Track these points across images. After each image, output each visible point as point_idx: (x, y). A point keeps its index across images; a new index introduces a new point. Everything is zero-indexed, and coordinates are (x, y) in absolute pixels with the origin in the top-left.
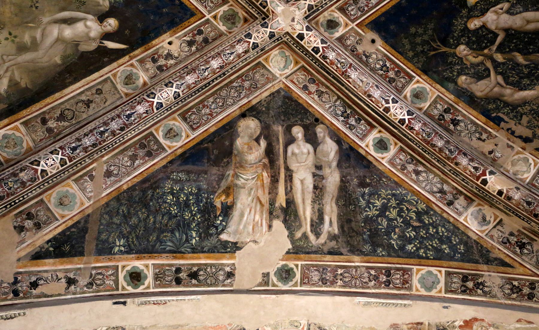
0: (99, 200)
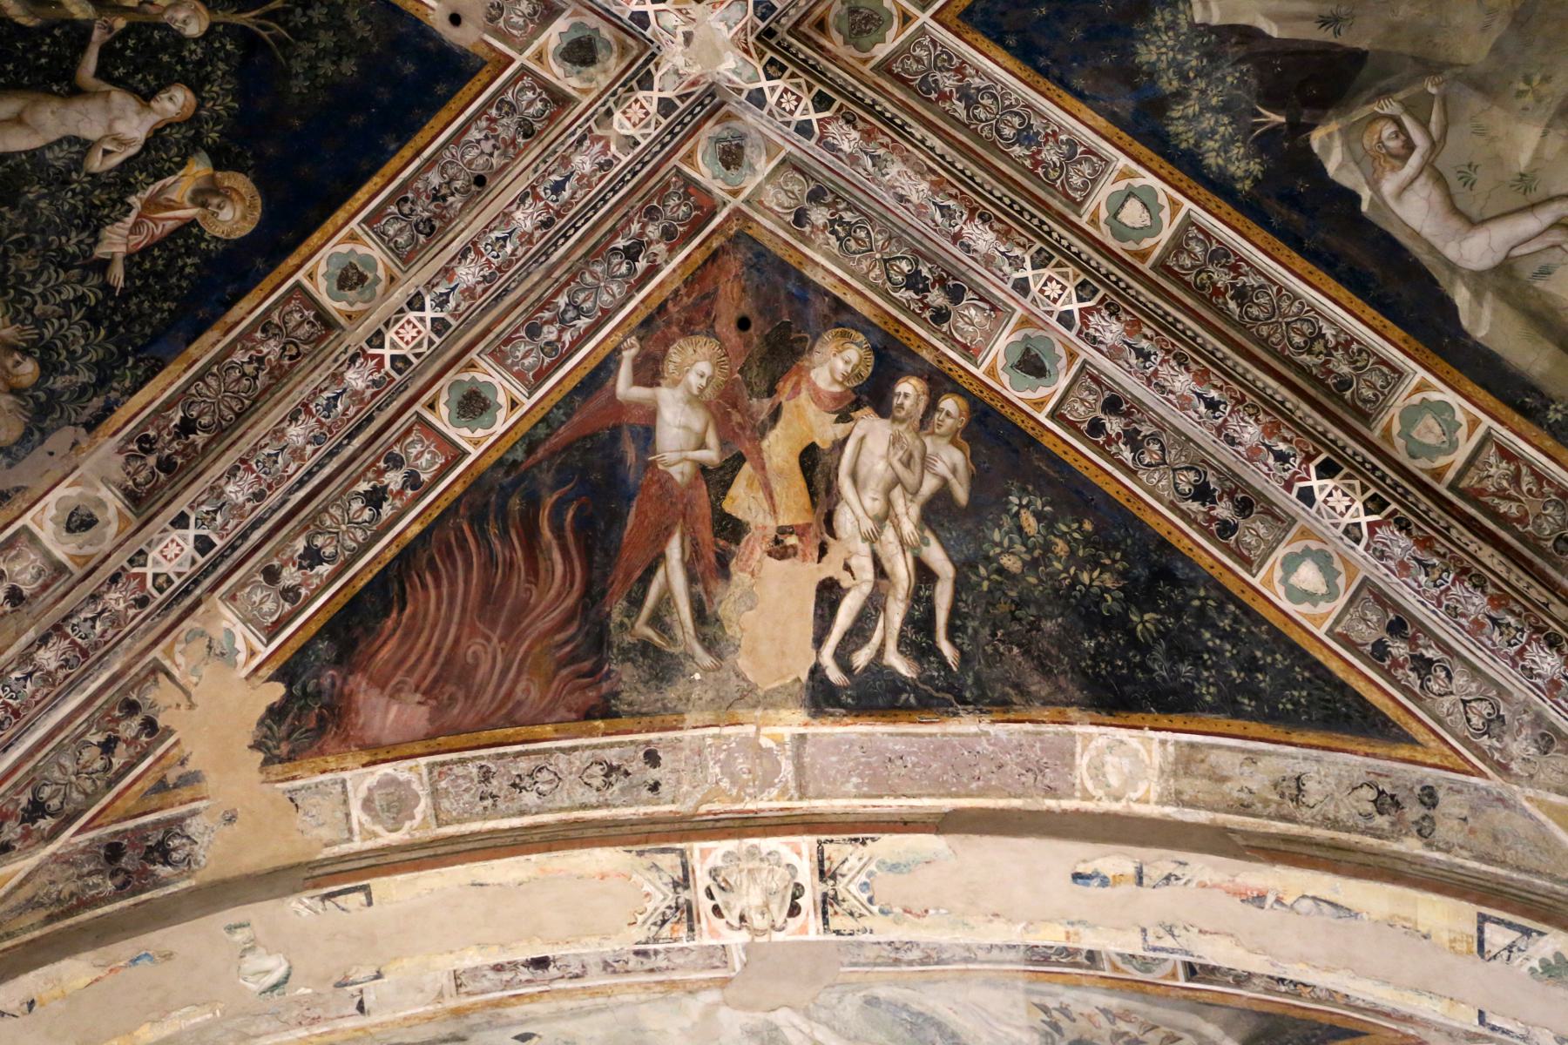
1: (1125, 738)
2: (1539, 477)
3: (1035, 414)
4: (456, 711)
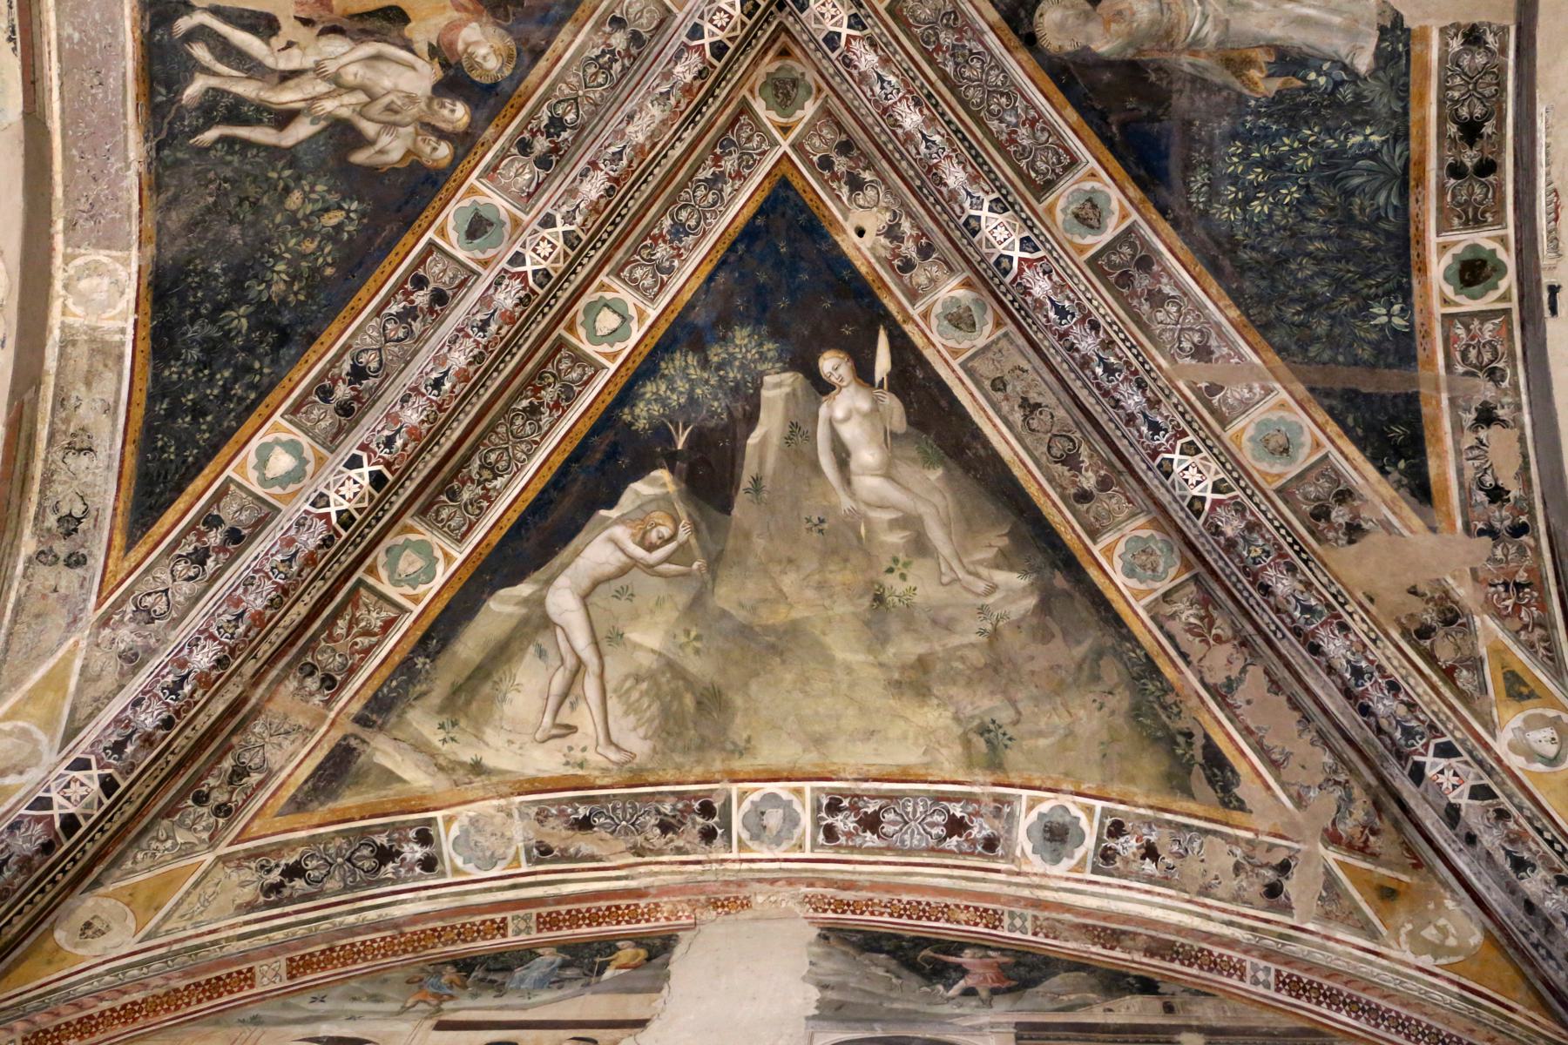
0: (1271, 370)
1: (126, 297)
2: (367, 651)
3: (433, 228)
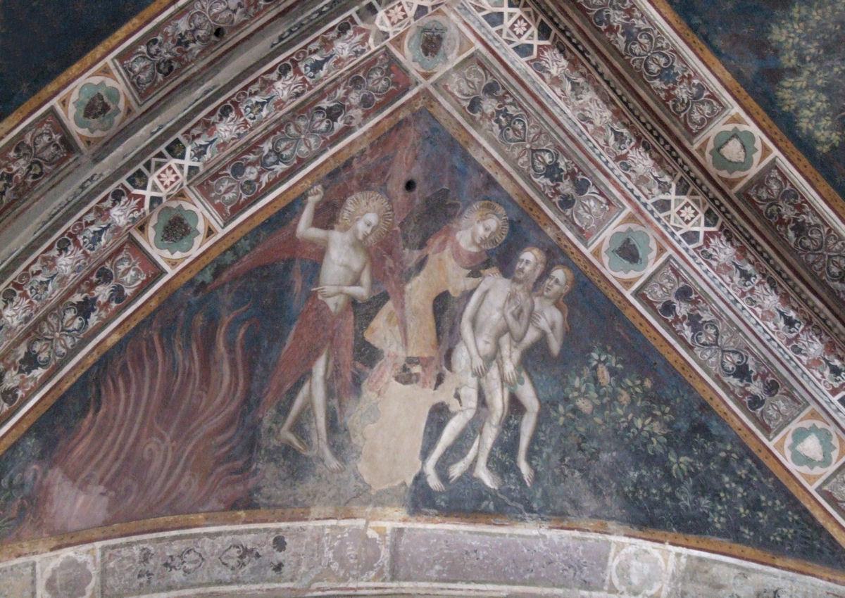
1: (649, 549)
4: (130, 501)
